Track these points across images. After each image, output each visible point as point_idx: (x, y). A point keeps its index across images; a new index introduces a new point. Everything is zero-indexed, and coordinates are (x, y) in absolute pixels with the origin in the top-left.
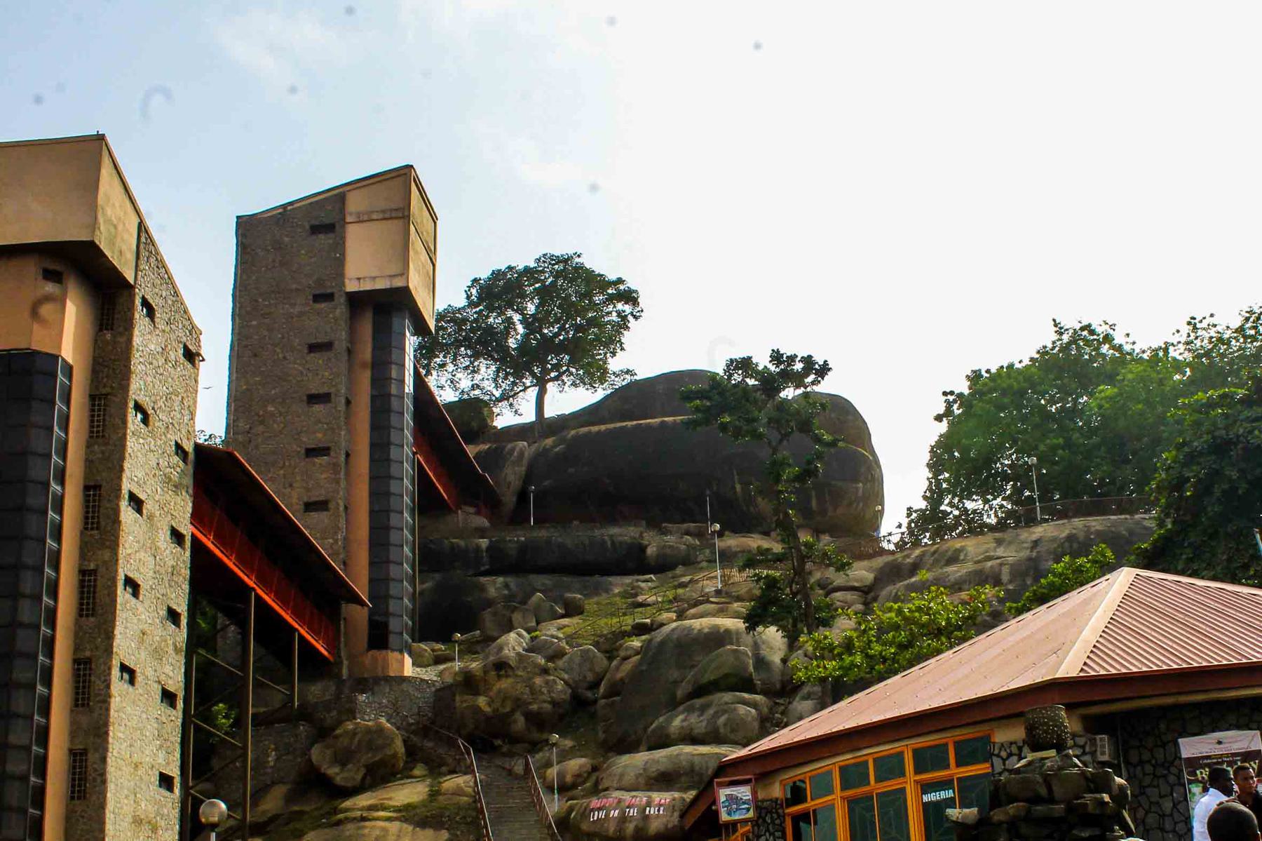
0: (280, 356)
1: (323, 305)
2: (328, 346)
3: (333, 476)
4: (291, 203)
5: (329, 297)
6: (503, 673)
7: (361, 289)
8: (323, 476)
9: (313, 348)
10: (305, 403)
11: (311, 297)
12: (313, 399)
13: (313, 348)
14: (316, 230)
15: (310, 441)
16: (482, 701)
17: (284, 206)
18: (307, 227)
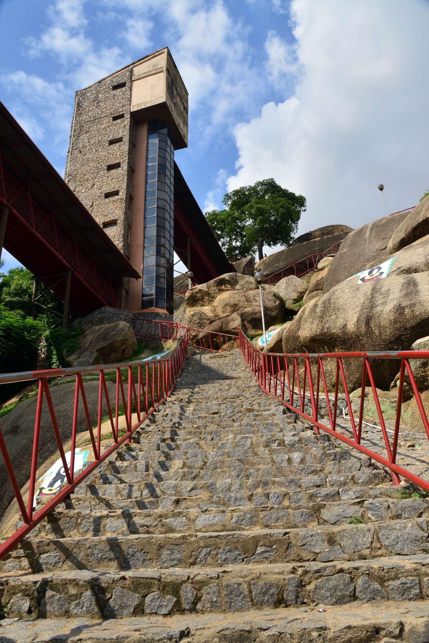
0: (94, 149)
1: (119, 121)
2: (120, 140)
3: (120, 206)
4: (104, 79)
5: (122, 116)
6: (223, 287)
7: (139, 108)
8: (115, 206)
9: (112, 142)
10: (105, 171)
11: (111, 119)
12: (110, 168)
13: (112, 142)
14: (115, 88)
15: (107, 189)
16: (207, 310)
17: (100, 82)
18: (111, 88)
